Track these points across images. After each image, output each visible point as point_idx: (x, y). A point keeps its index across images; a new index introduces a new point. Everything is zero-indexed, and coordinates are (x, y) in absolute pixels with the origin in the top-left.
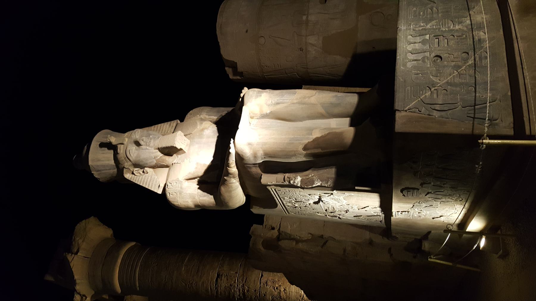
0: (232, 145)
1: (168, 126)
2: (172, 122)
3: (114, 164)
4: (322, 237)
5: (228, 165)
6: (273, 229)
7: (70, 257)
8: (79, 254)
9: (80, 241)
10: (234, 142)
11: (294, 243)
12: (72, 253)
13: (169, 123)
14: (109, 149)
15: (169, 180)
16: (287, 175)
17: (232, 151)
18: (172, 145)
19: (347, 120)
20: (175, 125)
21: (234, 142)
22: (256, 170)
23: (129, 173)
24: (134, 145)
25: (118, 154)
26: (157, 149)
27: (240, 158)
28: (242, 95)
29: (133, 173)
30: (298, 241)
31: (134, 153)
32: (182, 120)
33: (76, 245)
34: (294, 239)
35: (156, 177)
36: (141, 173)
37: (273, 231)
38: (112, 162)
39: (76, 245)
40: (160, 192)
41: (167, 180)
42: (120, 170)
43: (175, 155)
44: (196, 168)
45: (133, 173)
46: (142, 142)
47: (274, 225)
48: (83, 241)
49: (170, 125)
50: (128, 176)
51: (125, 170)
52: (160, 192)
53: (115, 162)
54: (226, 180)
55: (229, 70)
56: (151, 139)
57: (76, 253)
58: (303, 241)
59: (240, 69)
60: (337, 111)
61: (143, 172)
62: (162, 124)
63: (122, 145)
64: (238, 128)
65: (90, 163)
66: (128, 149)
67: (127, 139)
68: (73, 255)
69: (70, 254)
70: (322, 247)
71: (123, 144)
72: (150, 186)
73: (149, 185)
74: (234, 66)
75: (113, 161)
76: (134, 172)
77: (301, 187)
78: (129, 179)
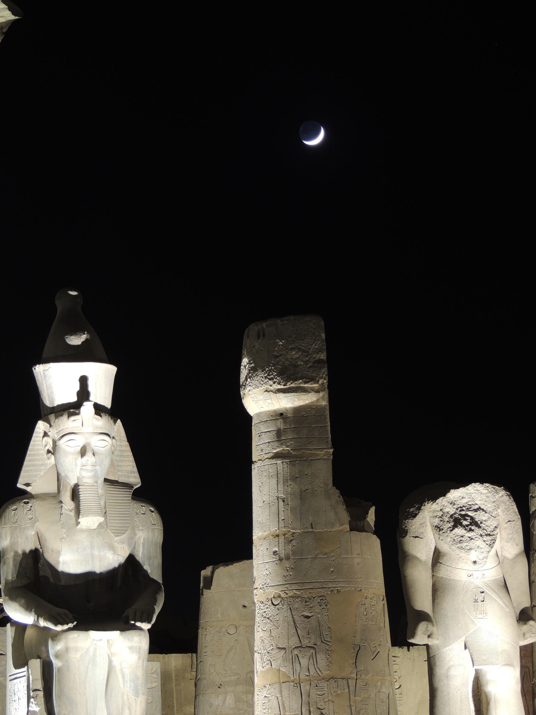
0: (66, 627)
1: (130, 468)
10: (70, 629)
13: (135, 469)
14: (79, 394)
16: (41, 694)
17: (59, 628)
21: (70, 629)
29: (46, 434)
32: (139, 495)
35: (42, 474)
36: (47, 448)
40: (19, 485)
44: (53, 551)
45: (46, 434)
50: (41, 426)
54: (31, 610)
61: (49, 452)
77: (28, 712)
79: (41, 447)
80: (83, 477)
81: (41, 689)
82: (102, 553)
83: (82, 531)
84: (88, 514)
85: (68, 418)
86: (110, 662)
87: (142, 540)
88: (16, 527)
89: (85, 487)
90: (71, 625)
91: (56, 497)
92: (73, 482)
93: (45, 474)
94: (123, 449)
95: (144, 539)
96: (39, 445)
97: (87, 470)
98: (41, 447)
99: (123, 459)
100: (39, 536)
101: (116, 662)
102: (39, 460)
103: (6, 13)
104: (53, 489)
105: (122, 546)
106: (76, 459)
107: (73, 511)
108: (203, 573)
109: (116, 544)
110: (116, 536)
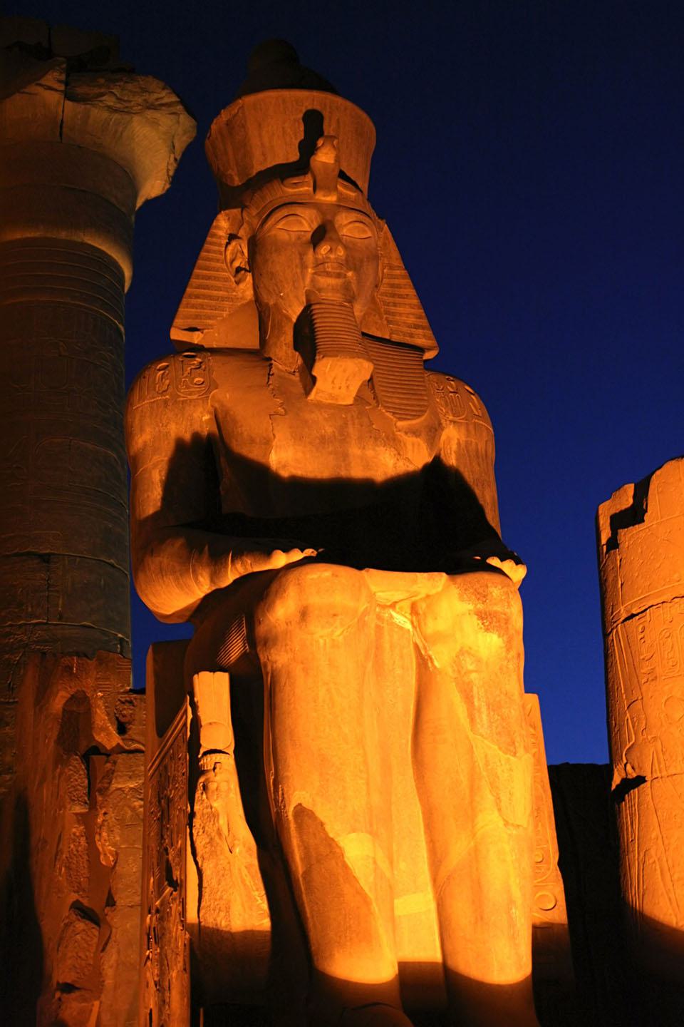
0: (297, 555)
1: (412, 320)
2: (429, 333)
3: (254, 172)
4: (111, 902)
5: (238, 555)
6: (122, 729)
7: (53, 78)
8: (69, 103)
9: (109, 100)
11: (78, 809)
12: (67, 84)
13: (425, 322)
15: (213, 361)
17: (280, 560)
18: (321, 348)
19: (427, 950)
20: (420, 341)
22: (236, 648)
23: (232, 225)
24: (315, 226)
25: (283, 180)
26: (308, 300)
27: (259, 590)
28: (495, 561)
29: (232, 237)
30: (87, 820)
31: (294, 227)
33: (97, 91)
34: (93, 805)
35: (225, 314)
36: (236, 264)
37: (112, 729)
38: (258, 166)
39: (97, 91)
40: (176, 334)
41: (213, 351)
42: (235, 198)
43: (300, 361)
44: (252, 441)
45: (232, 237)
46: (324, 249)
47: (134, 730)
48: (109, 107)
49: (417, 327)
50: (223, 224)
51: (236, 211)
52: (176, 334)
53: (260, 173)
54: (201, 552)
55: (626, 497)
56: (338, 276)
57: (69, 96)
58: (90, 836)
59: (628, 536)
60: (461, 911)
61: (238, 270)
62: (416, 301)
63: (311, 189)
64: (360, 568)
65: (249, 100)
66: (299, 210)
67: (332, 198)
68: (62, 87)
69: (63, 77)
70: (78, 908)
71: (315, 190)
72: (193, 301)
73: (197, 297)
74: (635, 515)
75: (262, 168)
76: (234, 243)
78: (213, 231)
79: (224, 266)
80: (320, 290)
81: (231, 751)
82: (370, 453)
83: (319, 406)
84: (338, 351)
85: (282, 182)
86: (423, 662)
87: (454, 447)
88: (166, 402)
89: (324, 306)
90: (309, 552)
91: (259, 356)
92: (295, 311)
93: (230, 315)
94: (396, 281)
95: (459, 444)
96: (218, 261)
97: (328, 274)
98: (224, 266)
99: (397, 300)
100: (221, 420)
101: (441, 658)
102: (219, 289)
103: (178, 107)
104: (251, 340)
105: (414, 439)
106: (302, 255)
107: (297, 374)
108: (606, 511)
109: (401, 435)
110: (400, 419)
